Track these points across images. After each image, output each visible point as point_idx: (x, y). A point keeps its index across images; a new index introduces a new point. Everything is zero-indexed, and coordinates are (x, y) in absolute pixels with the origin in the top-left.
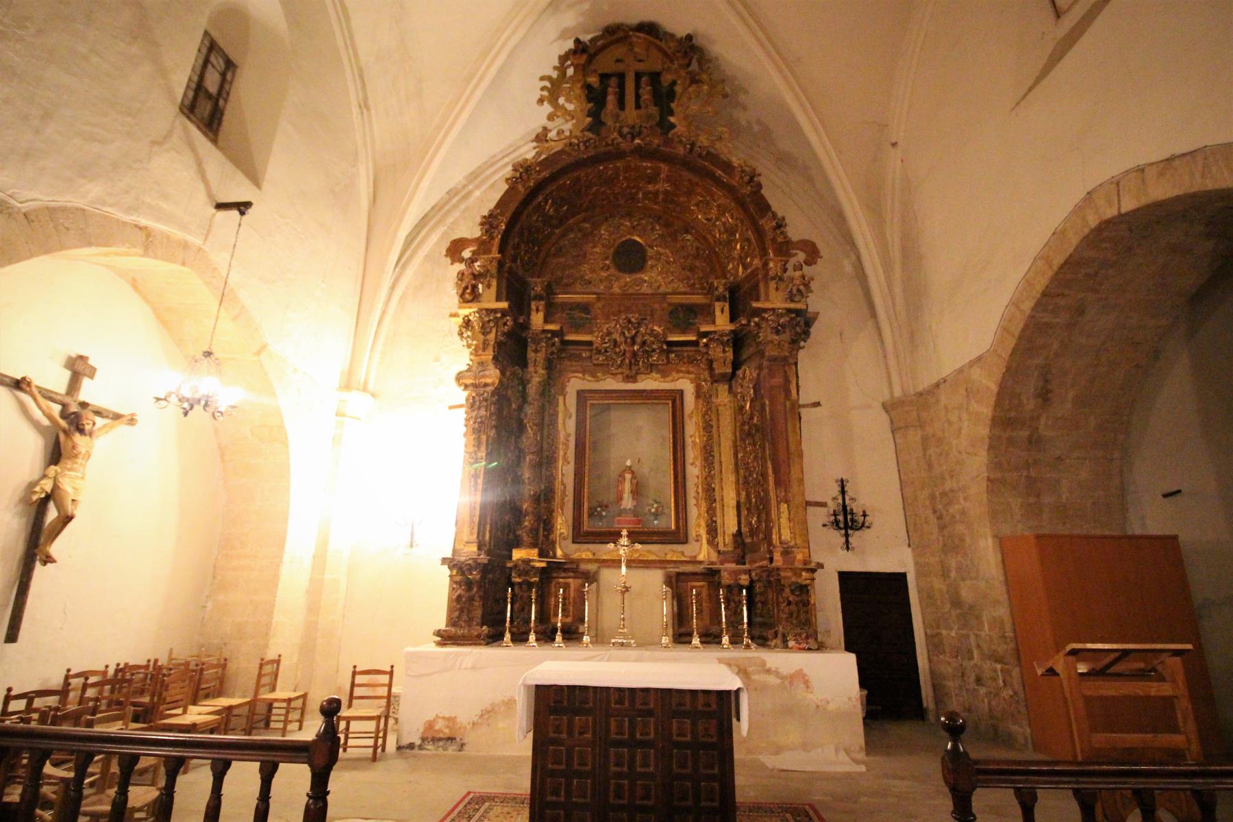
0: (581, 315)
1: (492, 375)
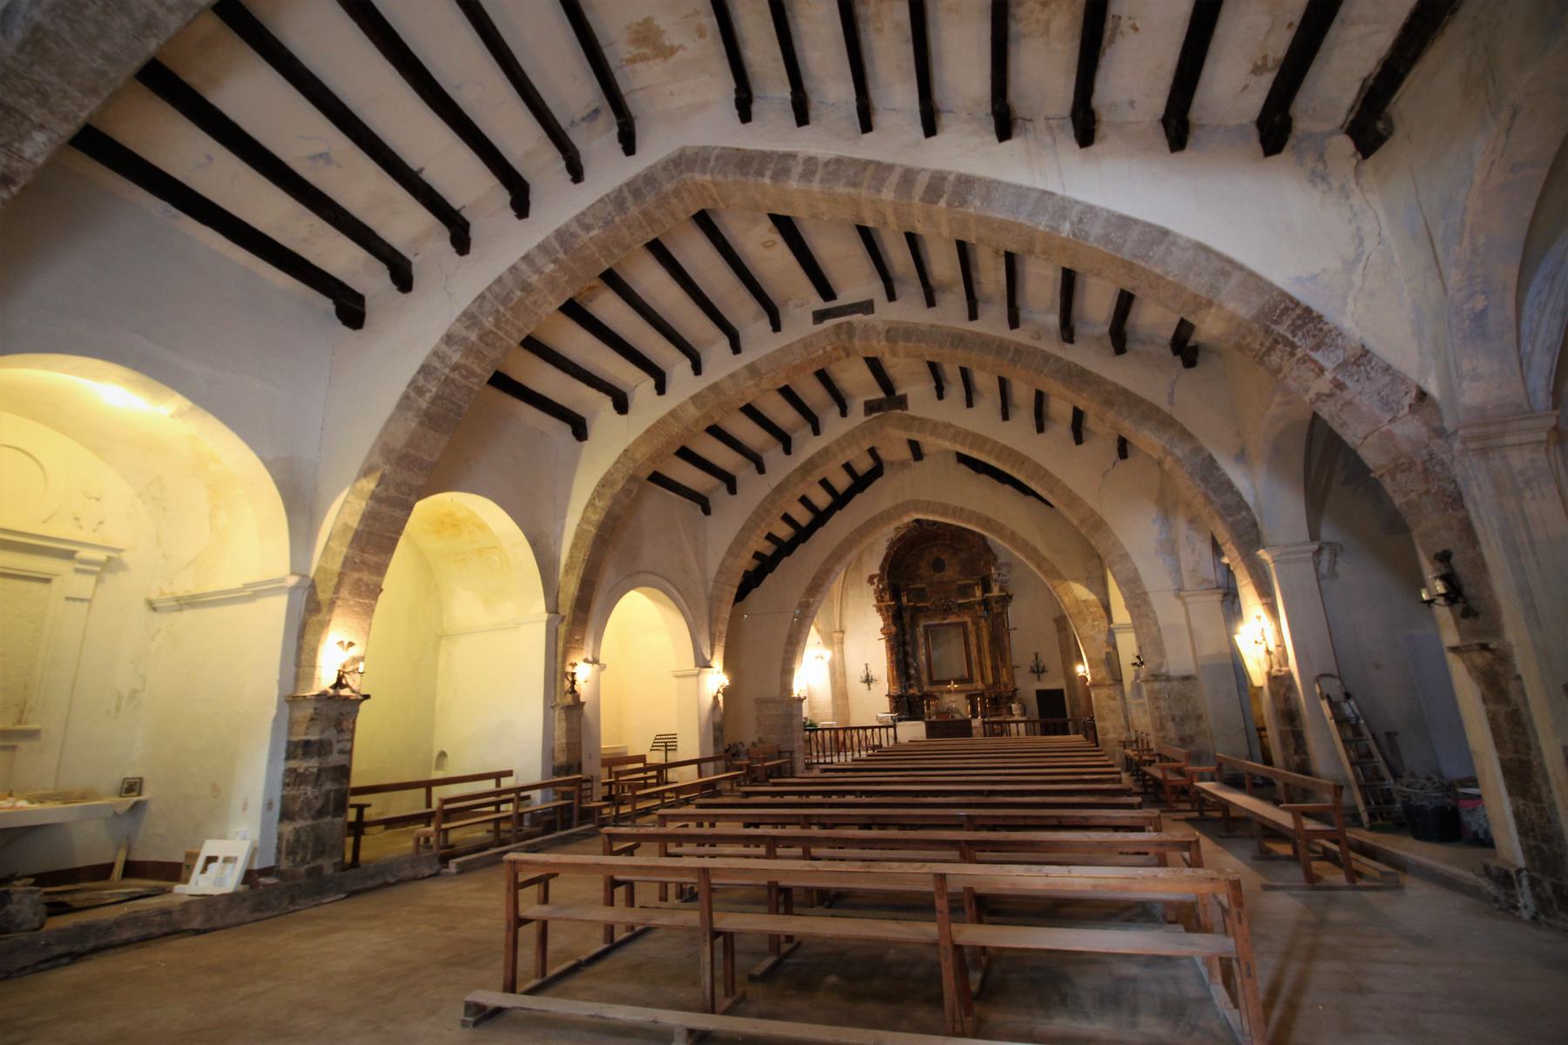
0: (921, 594)
1: (893, 629)
